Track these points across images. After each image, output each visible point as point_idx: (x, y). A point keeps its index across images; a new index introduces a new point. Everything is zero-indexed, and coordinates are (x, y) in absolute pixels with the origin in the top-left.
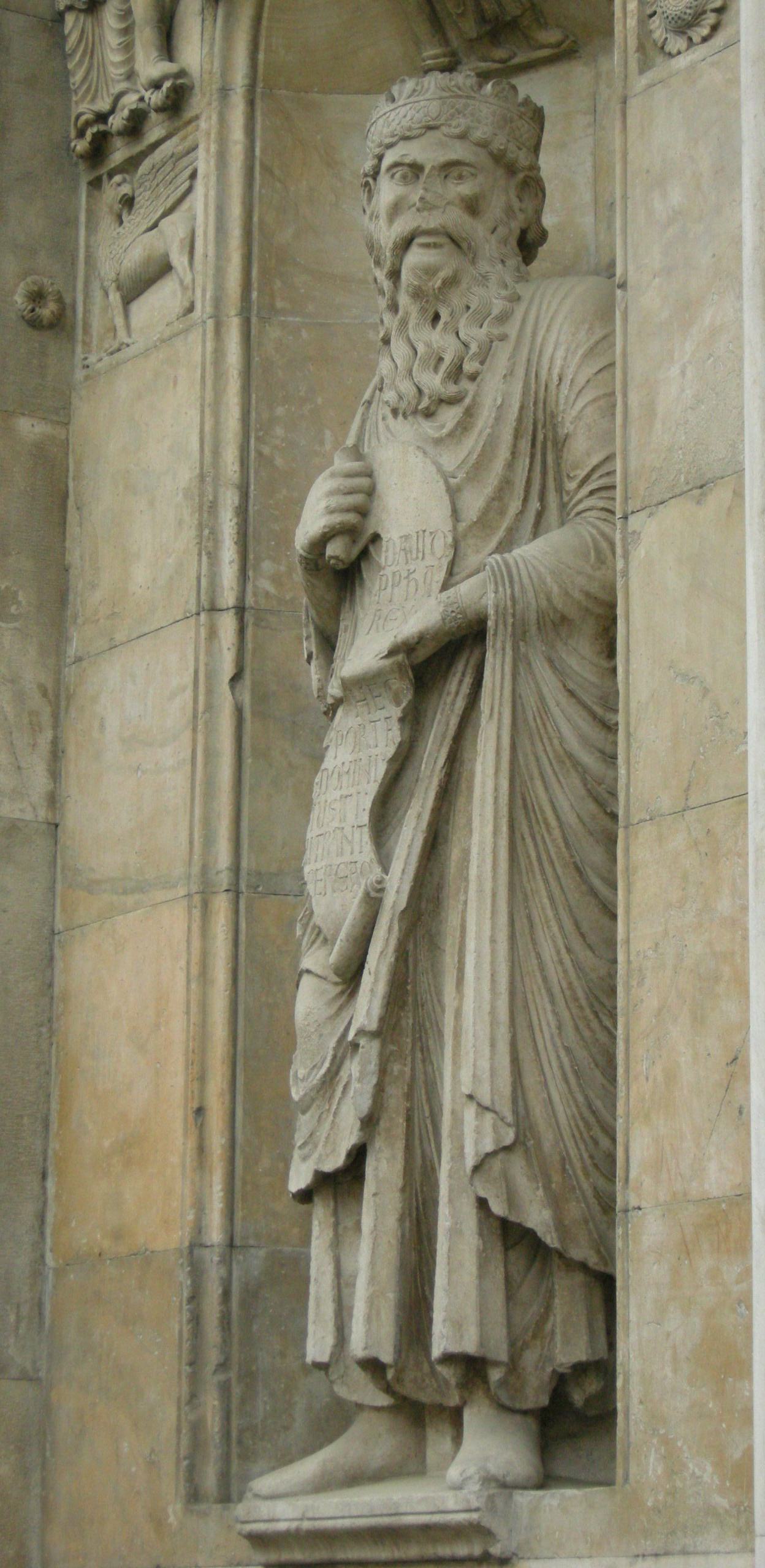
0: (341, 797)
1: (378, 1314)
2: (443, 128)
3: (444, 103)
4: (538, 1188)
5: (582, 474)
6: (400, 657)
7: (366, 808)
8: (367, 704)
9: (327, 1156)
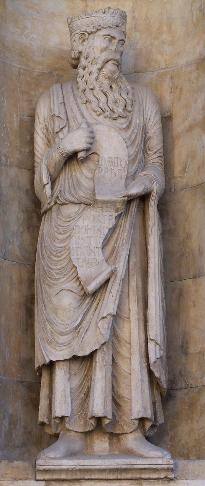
0: (88, 237)
1: (107, 403)
2: (120, 27)
3: (121, 19)
4: (163, 370)
5: (155, 151)
6: (126, 198)
7: (100, 242)
8: (102, 209)
9: (79, 351)
